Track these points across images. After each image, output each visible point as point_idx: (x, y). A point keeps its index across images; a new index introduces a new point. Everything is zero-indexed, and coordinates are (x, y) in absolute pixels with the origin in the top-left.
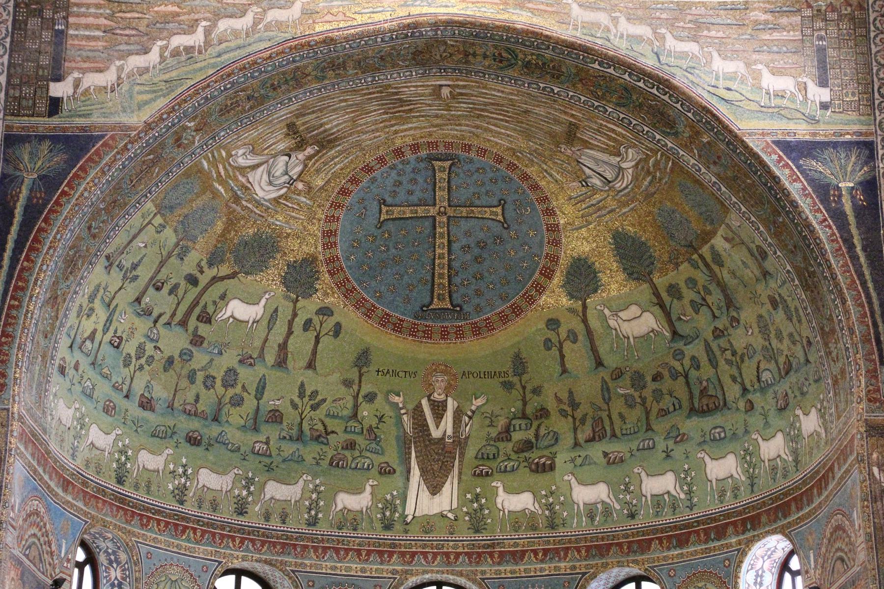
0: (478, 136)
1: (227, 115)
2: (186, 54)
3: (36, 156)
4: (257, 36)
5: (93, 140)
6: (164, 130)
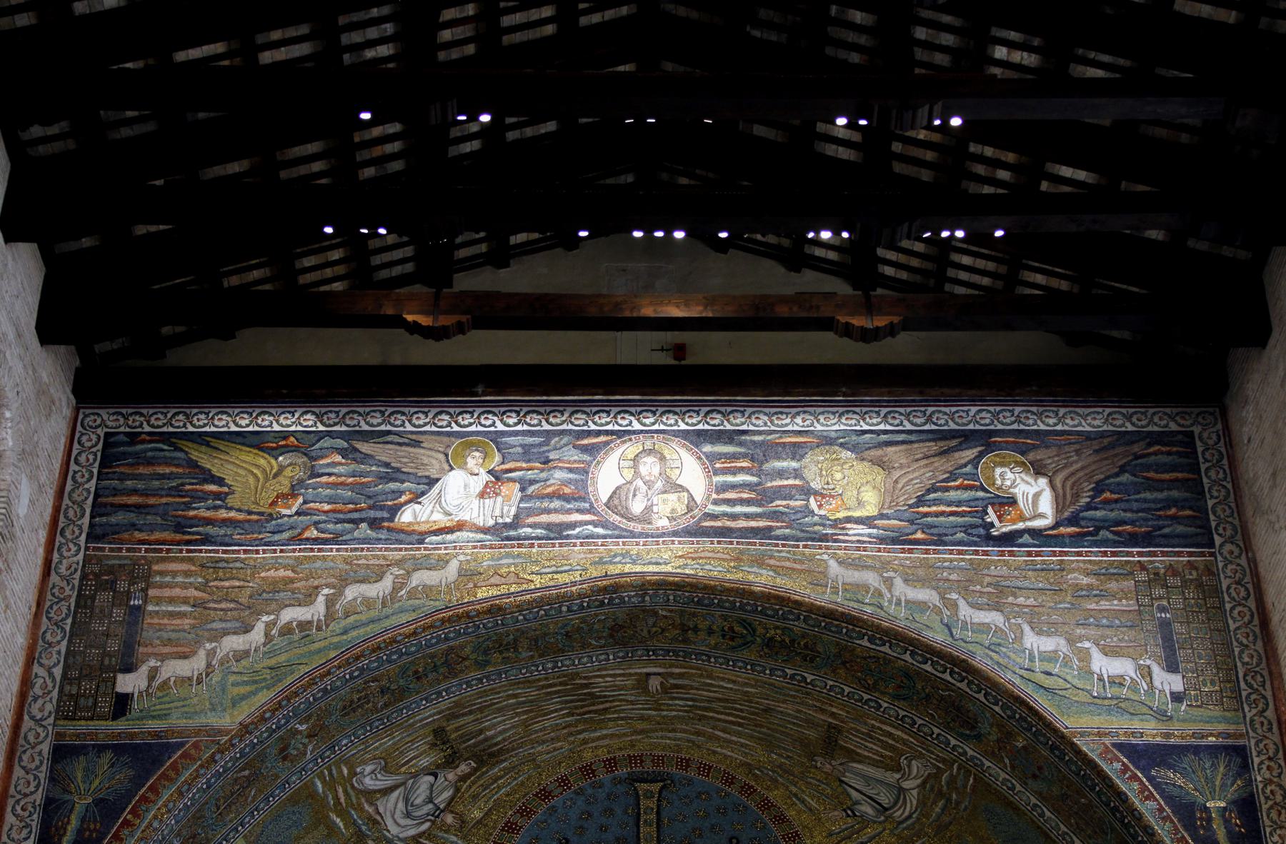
0: (699, 747)
1: (352, 714)
2: (300, 632)
3: (93, 773)
4: (397, 605)
5: (168, 749)
6: (265, 735)
